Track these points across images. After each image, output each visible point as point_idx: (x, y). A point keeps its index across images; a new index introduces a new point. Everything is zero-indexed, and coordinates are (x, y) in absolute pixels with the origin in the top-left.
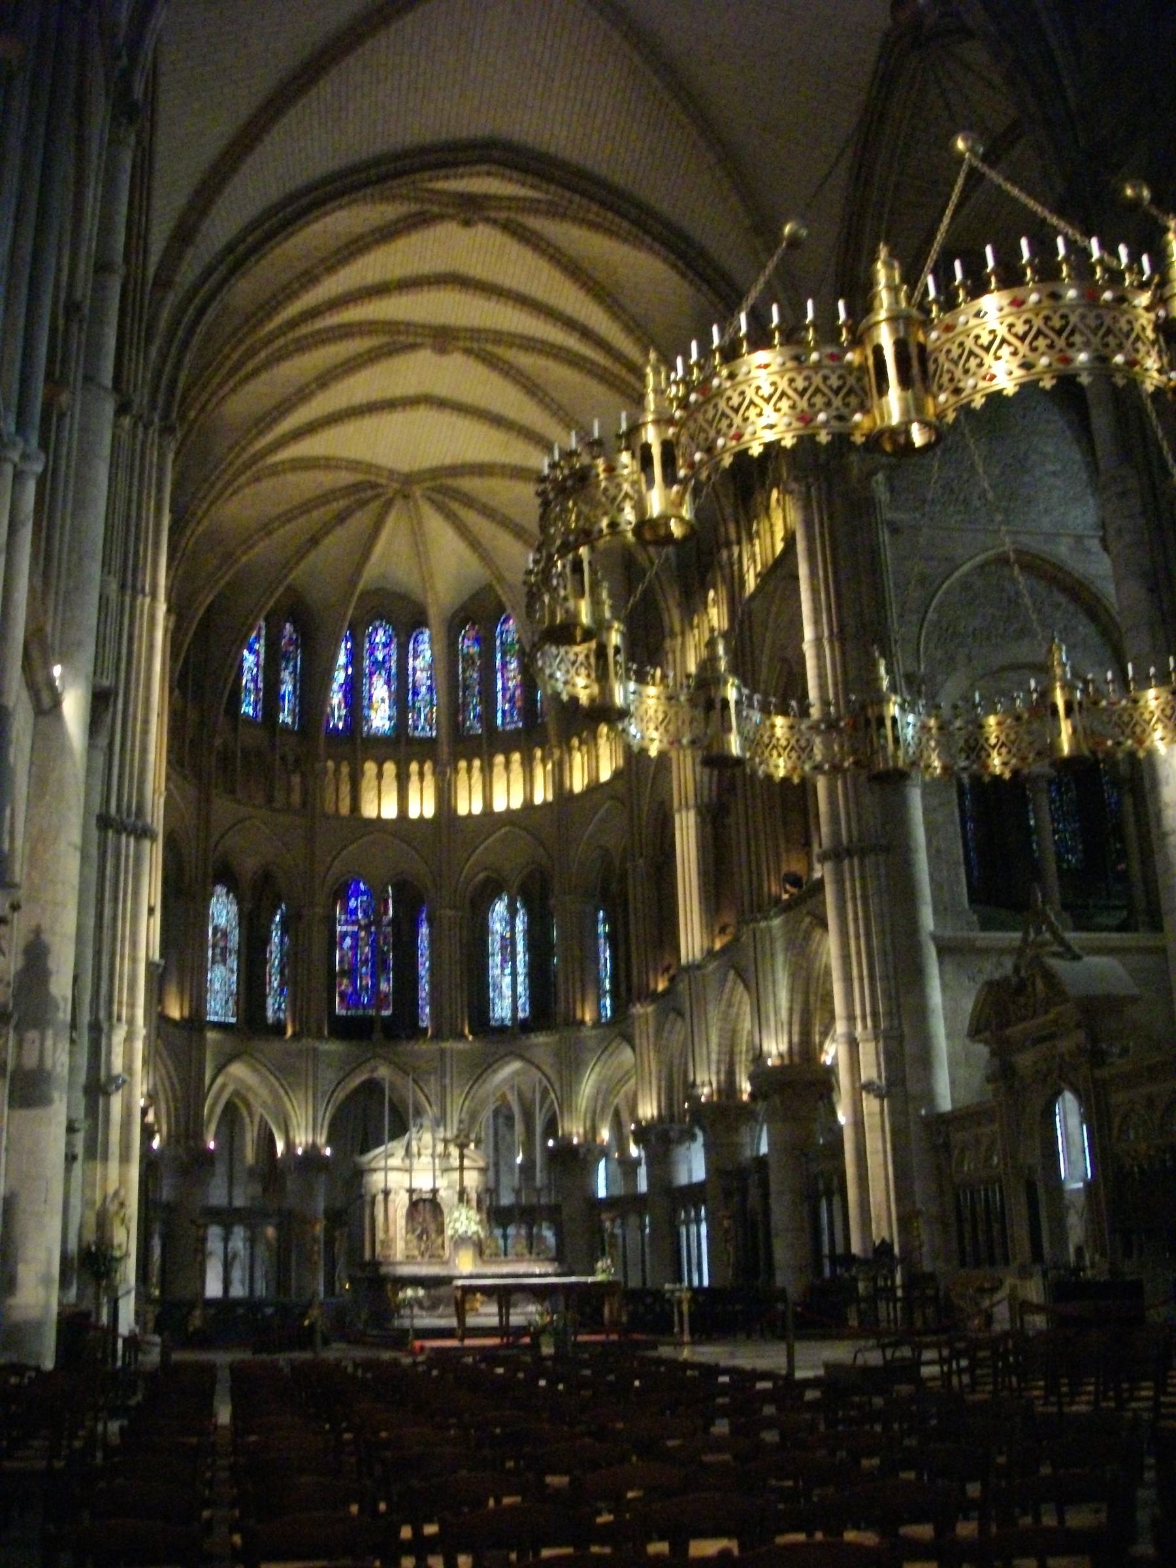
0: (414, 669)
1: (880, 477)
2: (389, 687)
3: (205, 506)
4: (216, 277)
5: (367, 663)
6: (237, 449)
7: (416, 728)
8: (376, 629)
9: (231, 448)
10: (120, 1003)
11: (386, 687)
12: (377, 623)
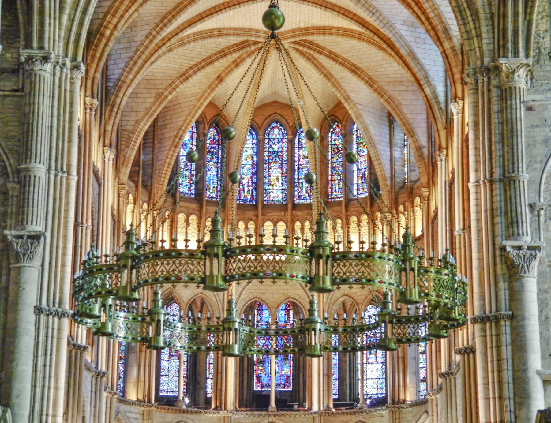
0: (299, 155)
1: (522, 72)
2: (282, 170)
3: (131, 77)
5: (266, 154)
6: (151, 37)
7: (300, 197)
8: (273, 128)
9: (147, 37)
10: (47, 415)
11: (280, 170)
12: (274, 125)
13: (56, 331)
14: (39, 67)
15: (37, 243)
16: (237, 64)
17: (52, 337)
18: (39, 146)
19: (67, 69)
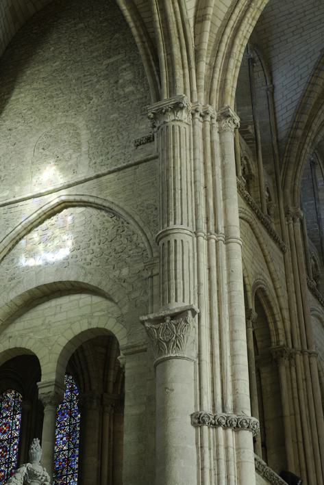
13: (232, 451)
14: (172, 117)
15: (183, 323)
17: (227, 461)
18: (178, 204)
19: (212, 118)
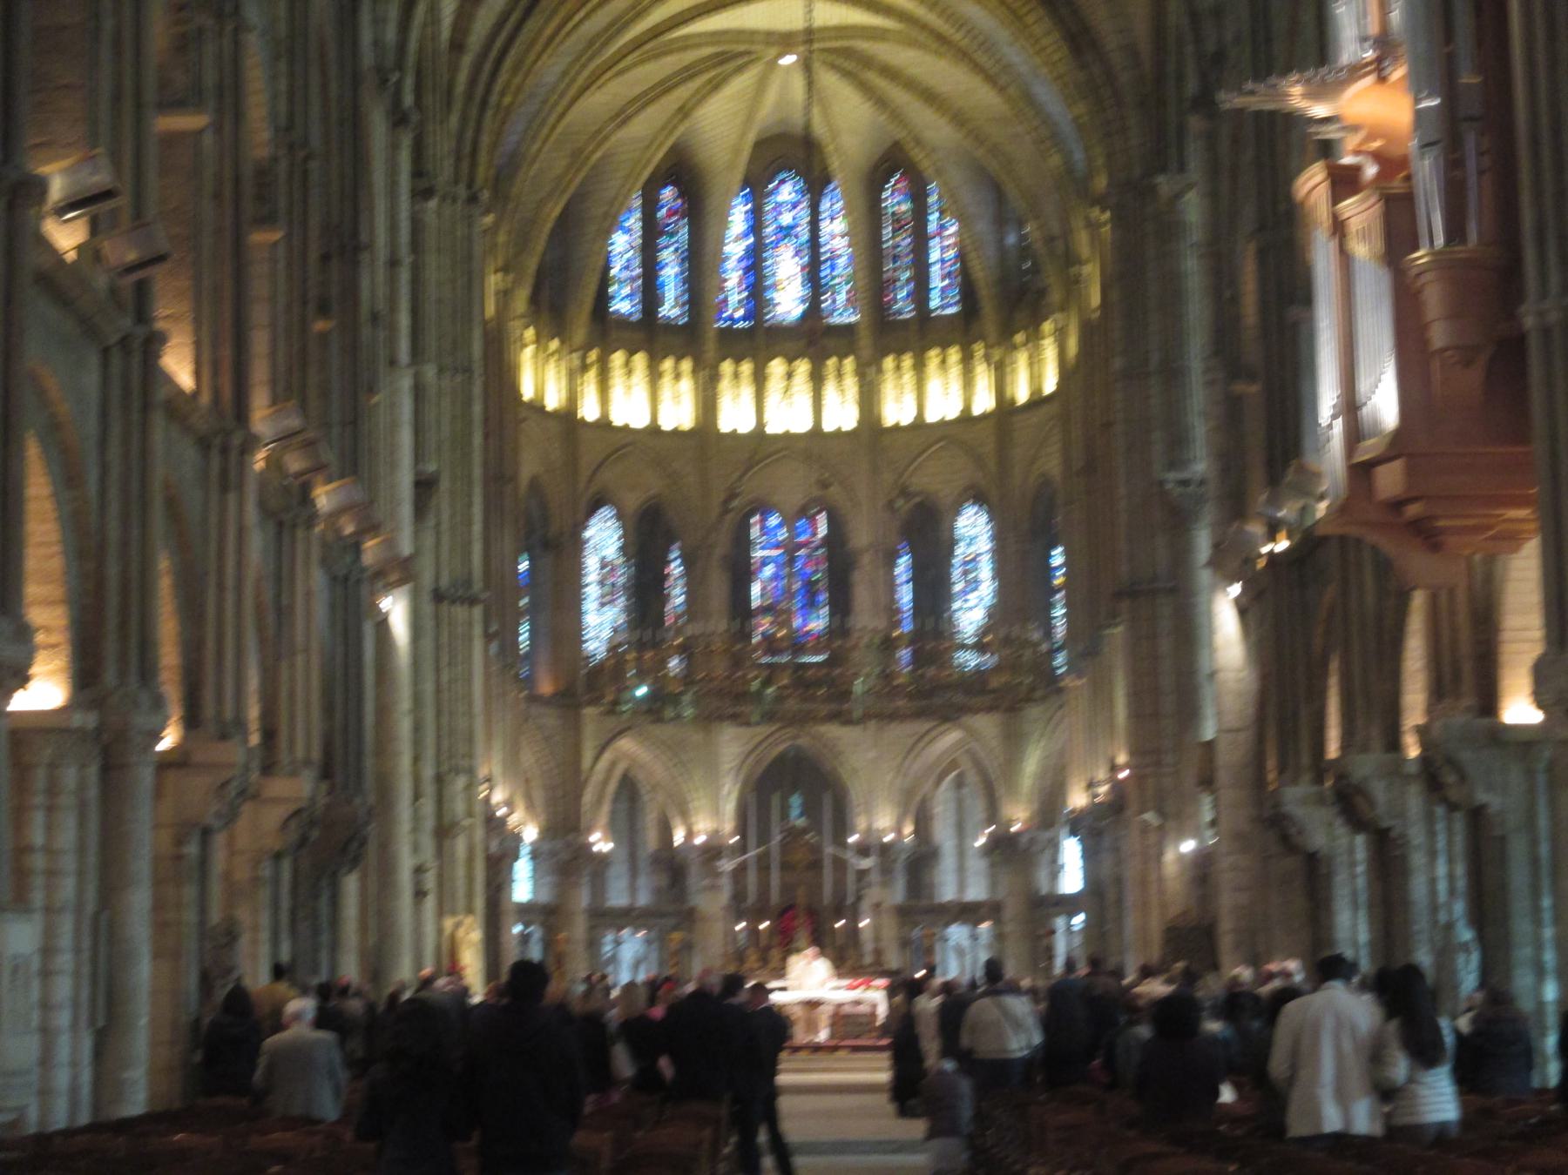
4: (509, 26)
8: (783, 182)
16: (715, 86)
